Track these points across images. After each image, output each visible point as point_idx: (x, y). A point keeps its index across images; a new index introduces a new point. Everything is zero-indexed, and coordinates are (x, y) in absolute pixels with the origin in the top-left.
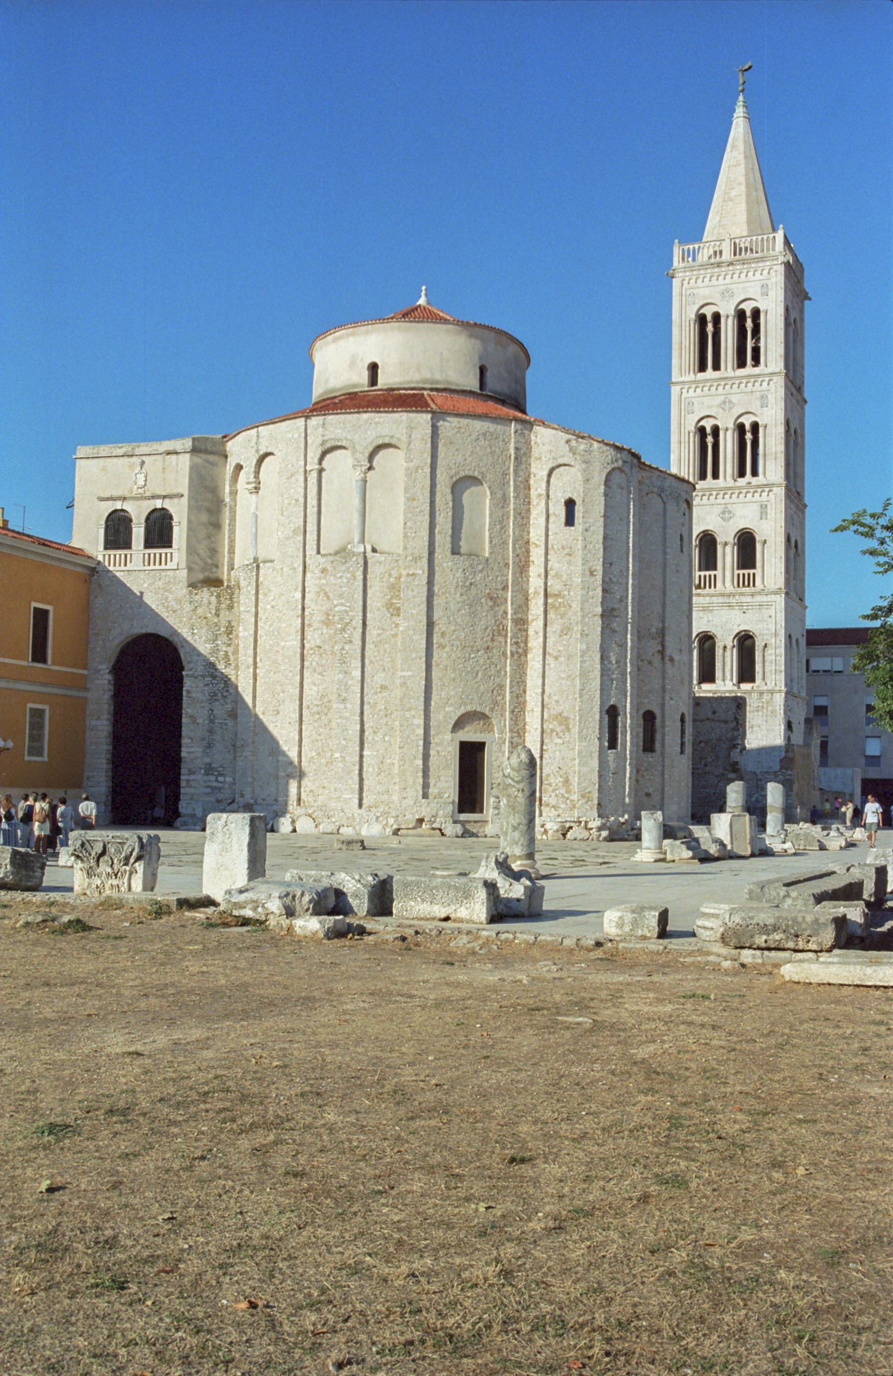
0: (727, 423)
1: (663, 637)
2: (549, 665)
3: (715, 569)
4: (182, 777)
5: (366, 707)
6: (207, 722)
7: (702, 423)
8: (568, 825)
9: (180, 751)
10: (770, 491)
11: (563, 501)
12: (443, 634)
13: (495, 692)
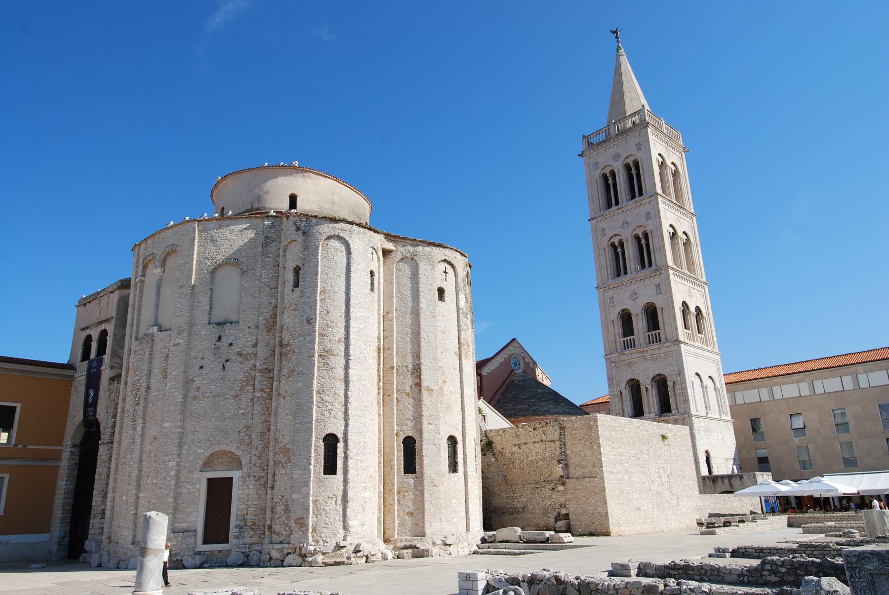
0: (627, 236)
1: (420, 372)
2: (280, 404)
3: (633, 335)
4: (91, 522)
5: (145, 456)
6: (106, 477)
7: (612, 240)
8: (286, 552)
9: (92, 501)
10: (661, 274)
11: (292, 268)
12: (198, 389)
13: (242, 434)
